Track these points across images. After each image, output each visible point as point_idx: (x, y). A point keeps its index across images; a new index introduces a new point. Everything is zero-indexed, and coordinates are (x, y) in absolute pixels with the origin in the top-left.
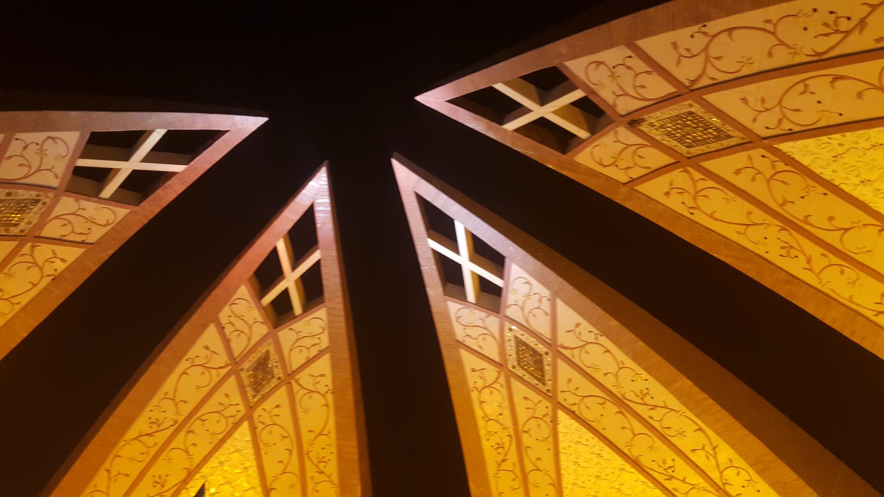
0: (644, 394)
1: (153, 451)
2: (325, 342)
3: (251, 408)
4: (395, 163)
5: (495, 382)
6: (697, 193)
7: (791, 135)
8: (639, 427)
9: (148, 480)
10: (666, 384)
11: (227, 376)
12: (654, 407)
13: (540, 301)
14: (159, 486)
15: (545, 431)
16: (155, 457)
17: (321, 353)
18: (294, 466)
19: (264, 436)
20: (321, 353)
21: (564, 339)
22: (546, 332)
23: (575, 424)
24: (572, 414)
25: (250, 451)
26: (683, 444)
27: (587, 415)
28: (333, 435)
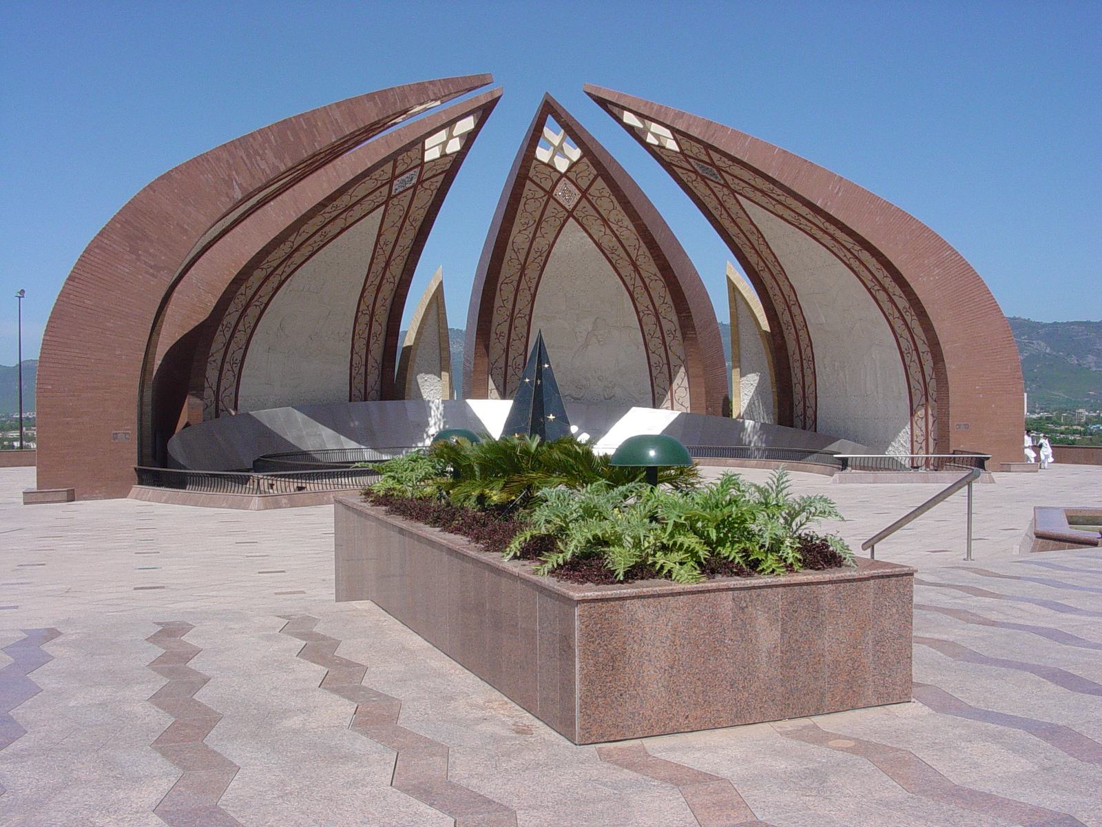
1: (327, 220)
2: (448, 166)
3: (390, 197)
5: (541, 198)
6: (695, 180)
7: (741, 194)
8: (608, 231)
9: (320, 233)
11: (387, 183)
12: (621, 227)
13: (589, 174)
14: (322, 237)
15: (558, 223)
18: (399, 224)
27: (584, 221)
28: (426, 209)
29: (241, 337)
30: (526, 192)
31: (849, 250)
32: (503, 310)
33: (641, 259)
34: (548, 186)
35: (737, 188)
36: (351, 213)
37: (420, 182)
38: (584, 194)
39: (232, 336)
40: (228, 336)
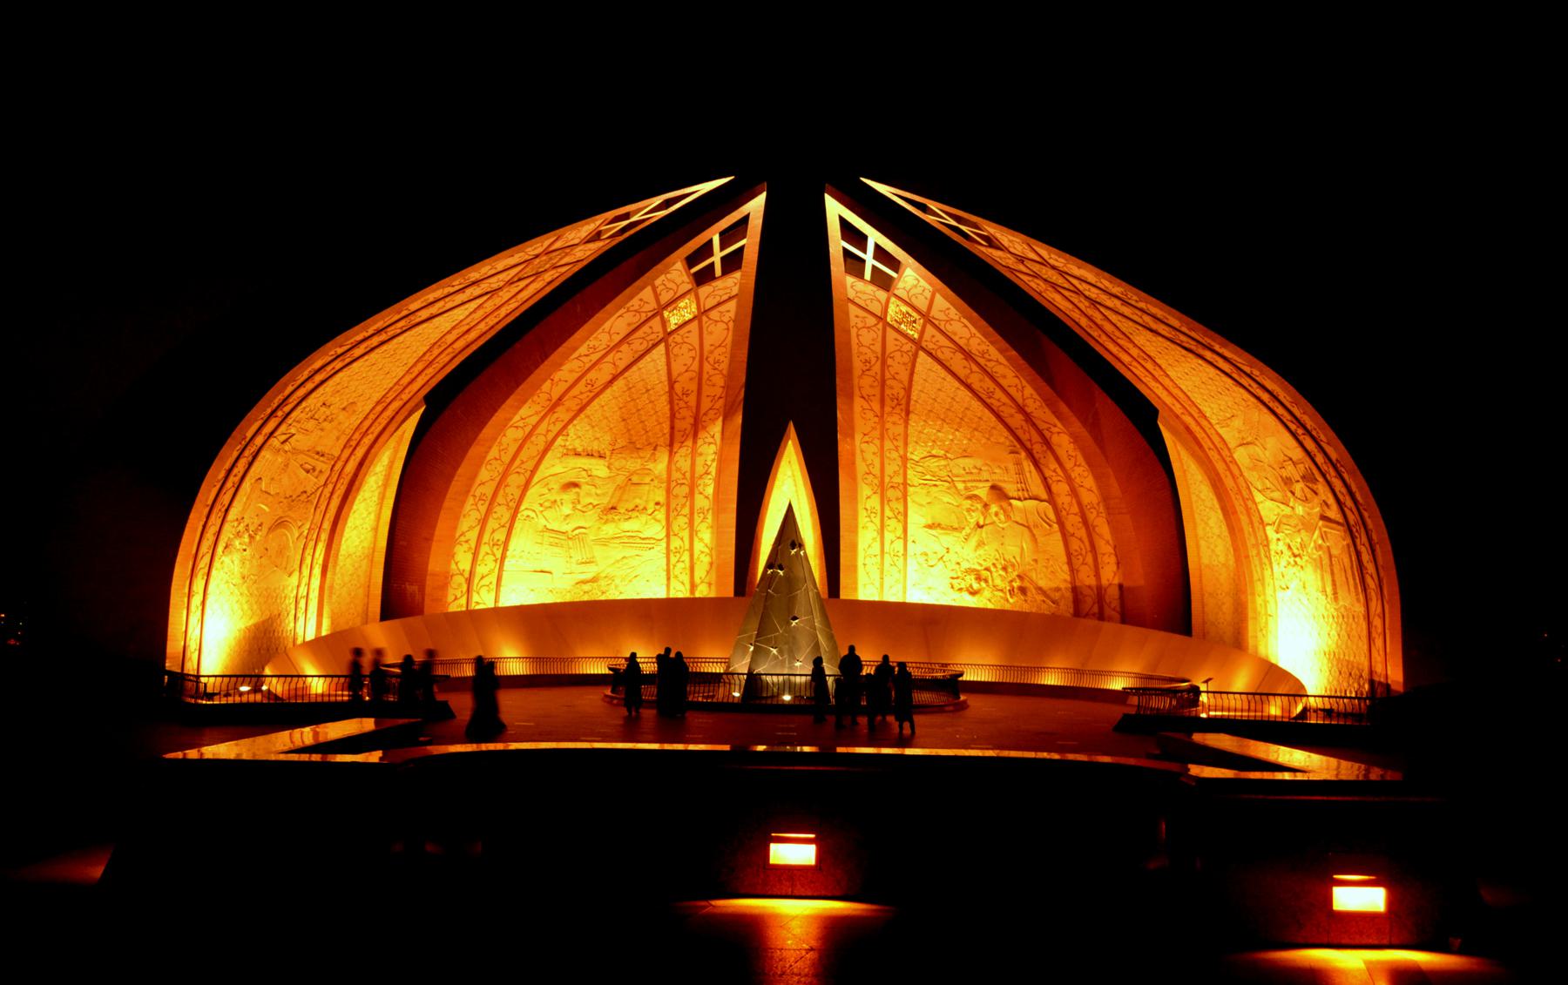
0: (983, 355)
4: (827, 198)
8: (975, 368)
9: (583, 382)
10: (1001, 351)
15: (906, 359)
16: (589, 369)
17: (730, 298)
18: (696, 366)
19: (676, 350)
20: (730, 298)
21: (934, 313)
22: (924, 308)
23: (930, 360)
24: (930, 354)
25: (664, 359)
26: (1004, 383)
27: (939, 355)
29: (502, 513)
30: (853, 321)
31: (1249, 376)
32: (870, 478)
33: (1030, 402)
34: (878, 312)
35: (1093, 296)
36: (619, 355)
37: (703, 313)
38: (926, 317)
39: (489, 512)
40: (483, 509)
